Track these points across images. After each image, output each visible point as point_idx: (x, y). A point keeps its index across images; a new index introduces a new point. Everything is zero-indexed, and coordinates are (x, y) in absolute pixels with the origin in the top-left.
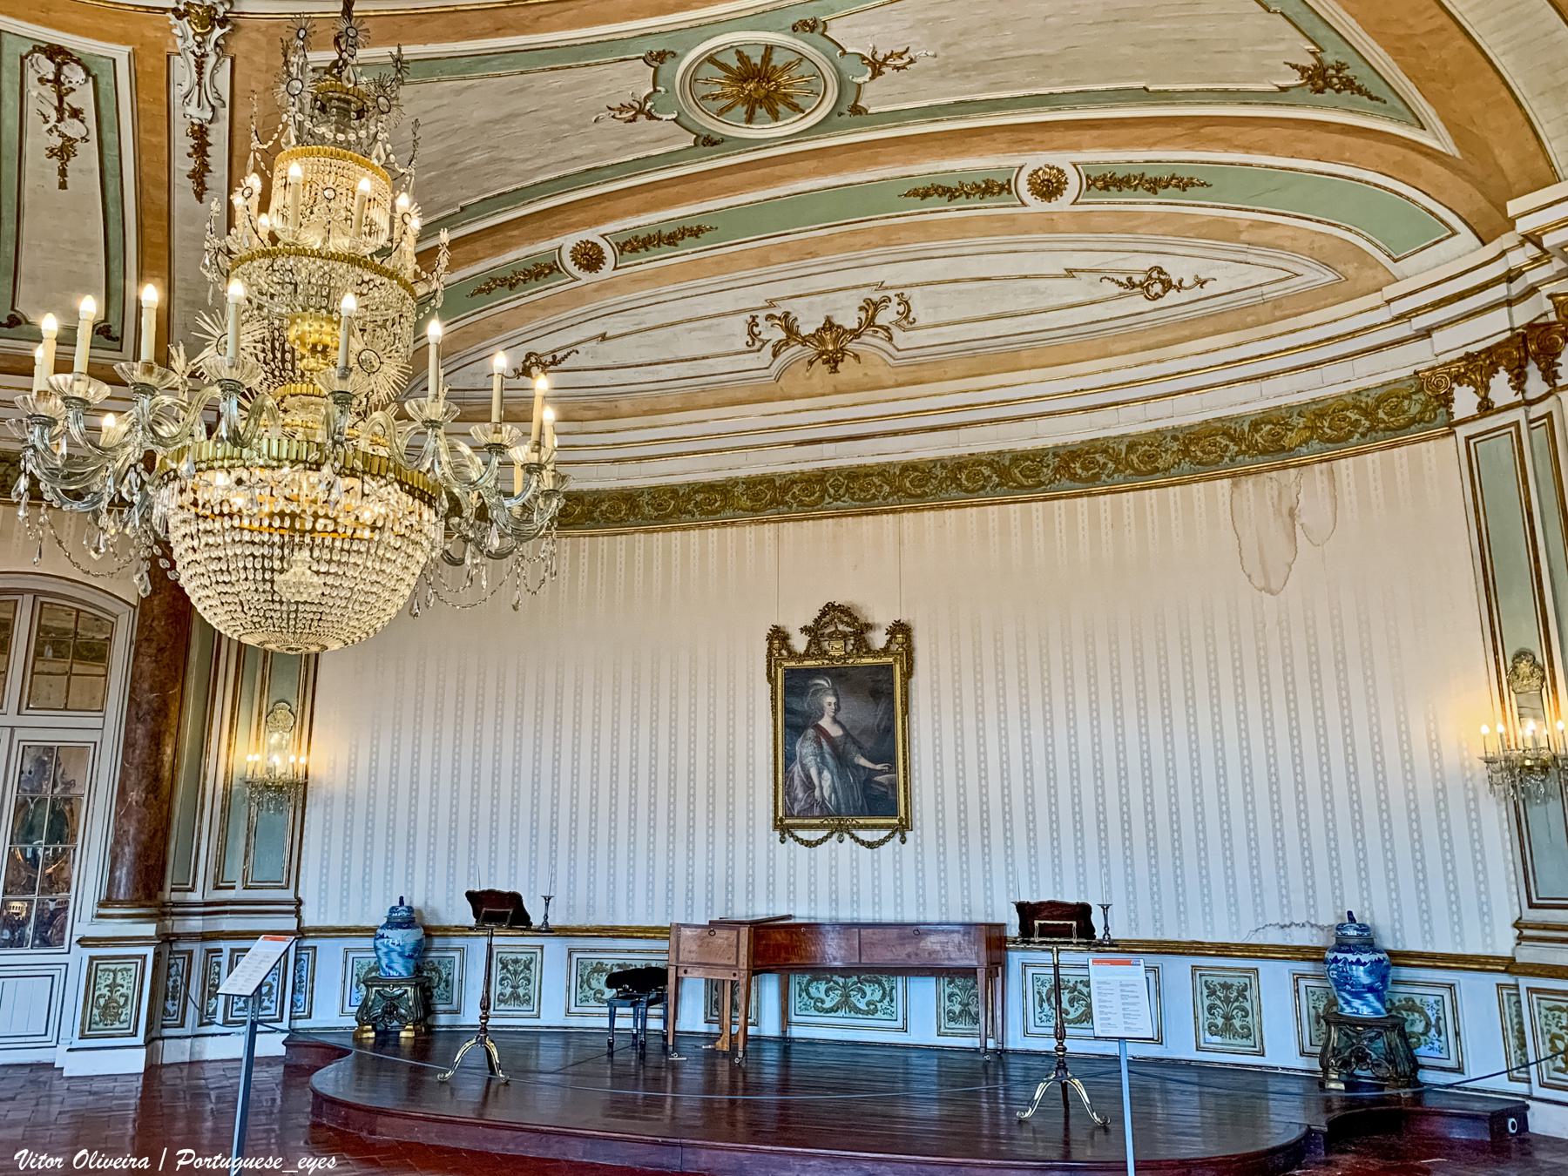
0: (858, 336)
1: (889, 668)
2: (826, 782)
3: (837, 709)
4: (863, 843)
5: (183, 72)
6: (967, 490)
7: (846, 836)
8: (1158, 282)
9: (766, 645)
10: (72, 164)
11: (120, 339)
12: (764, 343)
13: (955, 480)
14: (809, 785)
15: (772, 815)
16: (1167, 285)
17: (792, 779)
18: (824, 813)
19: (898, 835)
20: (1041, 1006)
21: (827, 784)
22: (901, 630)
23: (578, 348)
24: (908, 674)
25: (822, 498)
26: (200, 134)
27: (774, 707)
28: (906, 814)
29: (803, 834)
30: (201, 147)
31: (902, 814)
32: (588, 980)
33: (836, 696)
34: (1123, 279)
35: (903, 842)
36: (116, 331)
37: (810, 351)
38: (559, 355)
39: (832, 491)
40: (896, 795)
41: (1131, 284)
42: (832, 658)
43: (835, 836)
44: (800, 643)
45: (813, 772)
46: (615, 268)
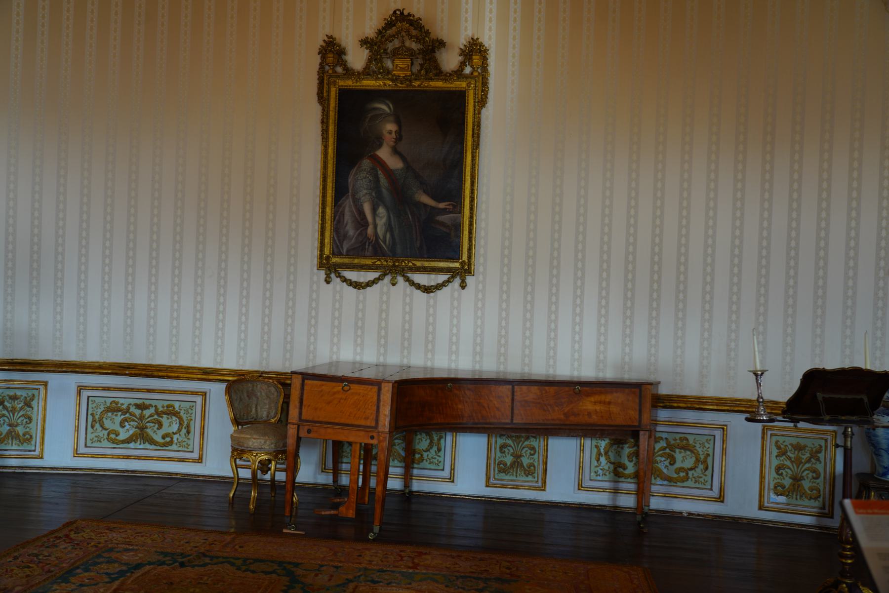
3: (399, 139)
4: (418, 287)
7: (400, 279)
9: (318, 59)
14: (361, 223)
15: (316, 253)
17: (343, 214)
18: (378, 252)
19: (457, 281)
20: (598, 460)
21: (381, 222)
24: (482, 102)
27: (325, 133)
28: (470, 257)
31: (465, 257)
32: (101, 420)
33: (398, 122)
35: (463, 286)
40: (459, 236)
42: (395, 79)
43: (387, 279)
44: (357, 58)
45: (367, 208)
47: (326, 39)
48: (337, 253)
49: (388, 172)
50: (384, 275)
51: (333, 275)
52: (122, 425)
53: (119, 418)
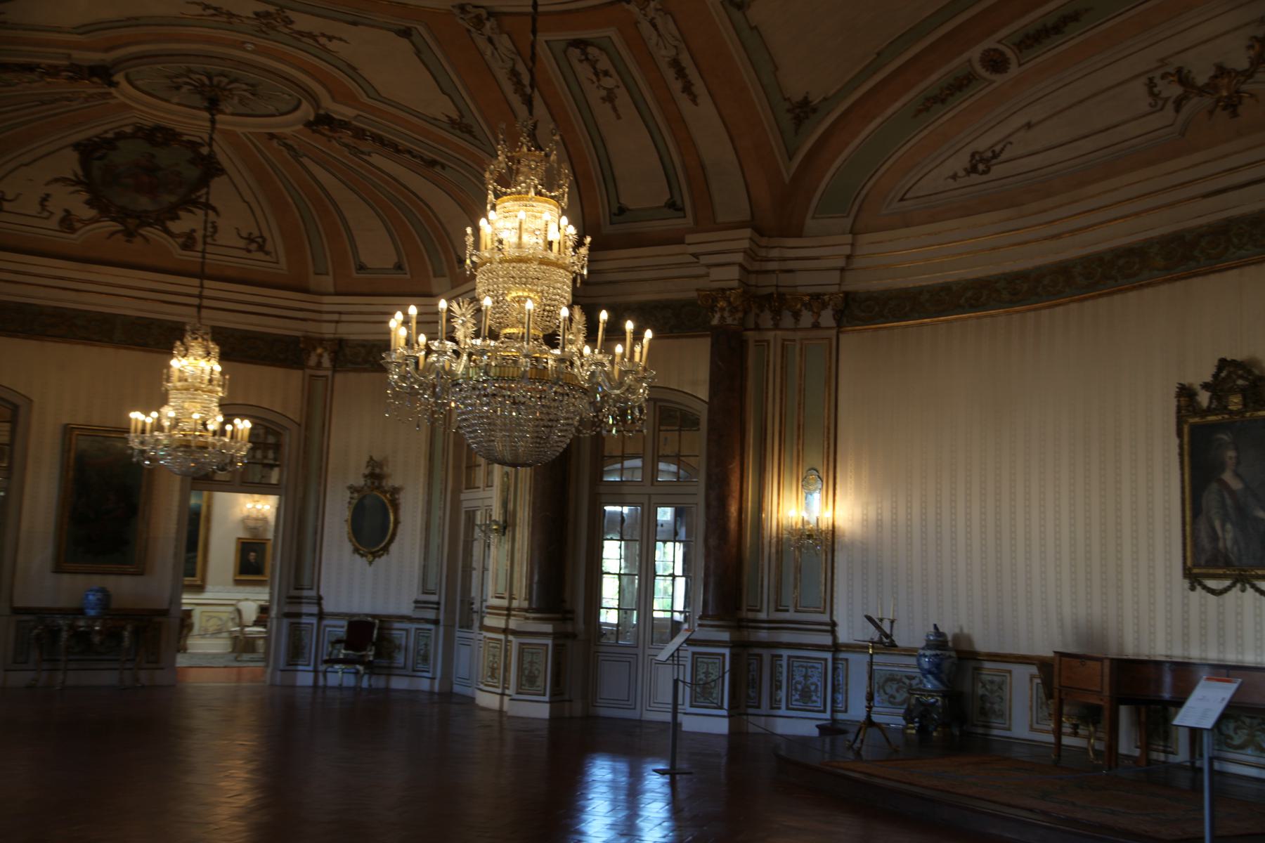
3: (1238, 463)
10: (617, 102)
11: (682, 209)
14: (1214, 538)
18: (1228, 564)
21: (1229, 536)
23: (1011, 139)
26: (676, 64)
29: (1211, 584)
30: (681, 72)
33: (1237, 449)
36: (679, 202)
37: (1208, 101)
38: (997, 149)
42: (1231, 413)
43: (1239, 585)
44: (1204, 398)
45: (1217, 524)
46: (1020, 65)
47: (1178, 386)
48: (1195, 565)
49: (1232, 493)
50: (1233, 585)
51: (1196, 584)
52: (897, 691)
53: (895, 686)
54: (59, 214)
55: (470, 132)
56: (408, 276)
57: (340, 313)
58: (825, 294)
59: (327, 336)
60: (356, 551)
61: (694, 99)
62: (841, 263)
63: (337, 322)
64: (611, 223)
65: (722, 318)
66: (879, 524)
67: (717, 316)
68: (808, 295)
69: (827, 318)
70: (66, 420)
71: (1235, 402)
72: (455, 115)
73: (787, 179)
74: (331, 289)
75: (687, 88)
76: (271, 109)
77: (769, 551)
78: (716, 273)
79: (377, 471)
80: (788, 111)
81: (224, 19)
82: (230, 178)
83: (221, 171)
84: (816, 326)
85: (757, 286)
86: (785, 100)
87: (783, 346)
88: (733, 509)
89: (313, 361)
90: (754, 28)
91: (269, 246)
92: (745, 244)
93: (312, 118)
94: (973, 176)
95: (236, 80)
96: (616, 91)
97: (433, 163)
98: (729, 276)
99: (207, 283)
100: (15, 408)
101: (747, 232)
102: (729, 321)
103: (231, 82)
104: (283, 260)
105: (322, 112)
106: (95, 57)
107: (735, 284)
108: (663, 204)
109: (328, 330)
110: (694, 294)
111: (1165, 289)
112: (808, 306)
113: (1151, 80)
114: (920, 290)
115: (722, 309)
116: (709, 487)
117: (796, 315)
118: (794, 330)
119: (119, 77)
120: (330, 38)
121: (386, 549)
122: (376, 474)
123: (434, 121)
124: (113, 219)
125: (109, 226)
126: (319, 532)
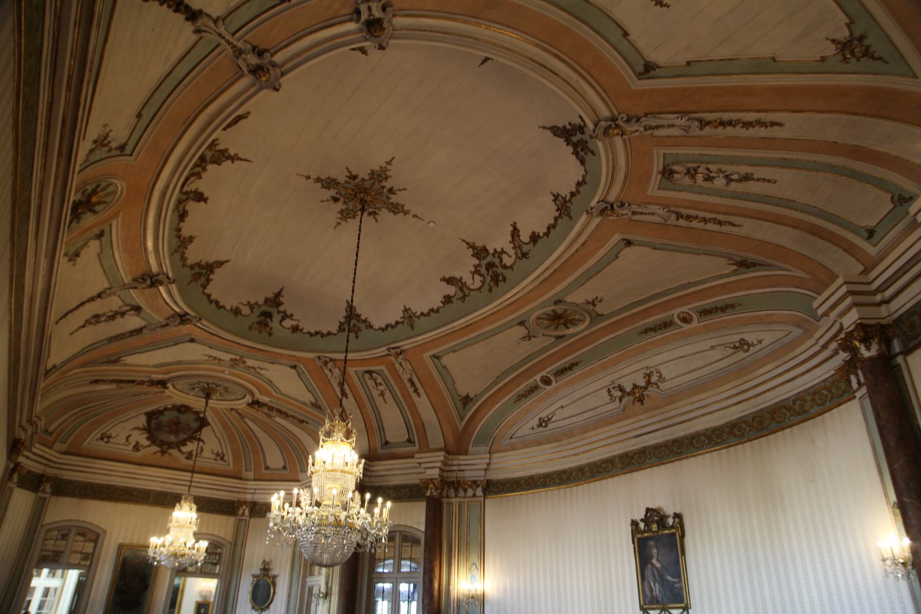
0: (647, 388)
1: (674, 534)
2: (657, 589)
5: (397, 366)
6: (697, 448)
8: (743, 345)
10: (385, 396)
11: (414, 442)
12: (616, 397)
13: (692, 444)
16: (750, 345)
22: (678, 516)
25: (645, 459)
26: (411, 380)
30: (413, 384)
34: (732, 346)
36: (412, 440)
37: (631, 398)
38: (550, 417)
39: (648, 456)
41: (735, 347)
42: (653, 532)
44: (642, 525)
54: (134, 443)
55: (320, 408)
56: (288, 472)
57: (255, 489)
58: (478, 481)
59: (248, 500)
60: (253, 608)
61: (419, 395)
62: (485, 466)
63: (254, 493)
64: (382, 448)
65: (431, 492)
66: (505, 591)
67: (429, 492)
68: (470, 481)
69: (479, 492)
70: (120, 541)
71: (654, 527)
72: (313, 401)
73: (460, 430)
74: (252, 477)
75: (416, 391)
76: (233, 398)
77: (453, 605)
78: (428, 472)
79: (267, 567)
80: (460, 400)
81: (217, 361)
82: (212, 427)
83: (208, 424)
84: (474, 495)
85: (447, 477)
86: (458, 395)
87: (459, 505)
88: (436, 585)
89: (241, 512)
90: (444, 367)
91: (226, 458)
92: (442, 458)
93: (250, 401)
94: (540, 428)
95: (219, 386)
96: (385, 391)
97: (303, 421)
98: (434, 473)
99: (195, 475)
100: (98, 535)
101: (443, 453)
102: (434, 493)
103: (217, 387)
104: (231, 464)
105: (255, 399)
106: (160, 377)
107: (437, 476)
108: (405, 440)
109: (249, 497)
110: (418, 481)
111: (622, 477)
112: (471, 486)
113: (609, 389)
114: (520, 479)
115: (432, 488)
116: (425, 574)
117: (465, 491)
118: (465, 497)
119: (169, 385)
120: (261, 369)
121: (268, 607)
122: (266, 569)
123: (304, 403)
124: (157, 446)
125: (155, 448)
126: (236, 598)
